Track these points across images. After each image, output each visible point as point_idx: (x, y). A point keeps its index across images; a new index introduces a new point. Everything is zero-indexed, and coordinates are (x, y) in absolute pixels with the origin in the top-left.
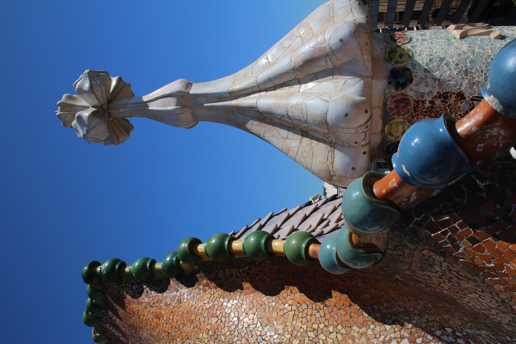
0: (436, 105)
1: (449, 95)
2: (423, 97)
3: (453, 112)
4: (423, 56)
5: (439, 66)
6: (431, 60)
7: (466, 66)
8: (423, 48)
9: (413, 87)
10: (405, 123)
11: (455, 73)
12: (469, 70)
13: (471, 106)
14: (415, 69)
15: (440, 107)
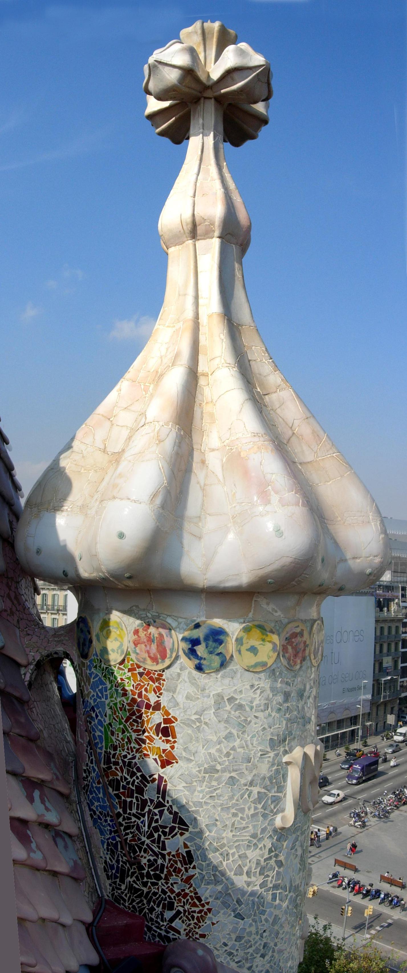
0: (152, 714)
1: (170, 738)
2: (167, 690)
3: (140, 745)
4: (251, 694)
5: (227, 721)
6: (240, 707)
7: (224, 771)
8: (268, 692)
9: (187, 672)
10: (121, 655)
11: (213, 751)
12: (216, 775)
13: (150, 776)
14: (223, 677)
15: (148, 721)
